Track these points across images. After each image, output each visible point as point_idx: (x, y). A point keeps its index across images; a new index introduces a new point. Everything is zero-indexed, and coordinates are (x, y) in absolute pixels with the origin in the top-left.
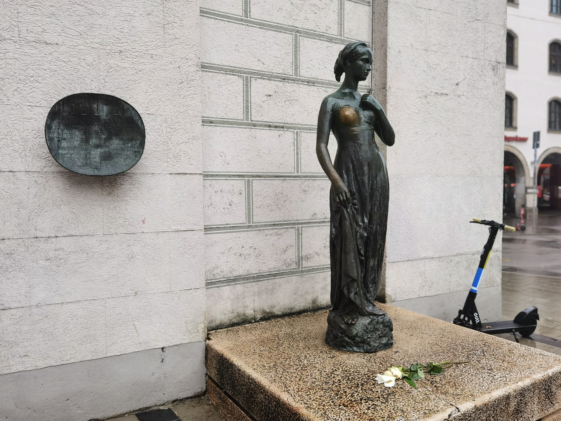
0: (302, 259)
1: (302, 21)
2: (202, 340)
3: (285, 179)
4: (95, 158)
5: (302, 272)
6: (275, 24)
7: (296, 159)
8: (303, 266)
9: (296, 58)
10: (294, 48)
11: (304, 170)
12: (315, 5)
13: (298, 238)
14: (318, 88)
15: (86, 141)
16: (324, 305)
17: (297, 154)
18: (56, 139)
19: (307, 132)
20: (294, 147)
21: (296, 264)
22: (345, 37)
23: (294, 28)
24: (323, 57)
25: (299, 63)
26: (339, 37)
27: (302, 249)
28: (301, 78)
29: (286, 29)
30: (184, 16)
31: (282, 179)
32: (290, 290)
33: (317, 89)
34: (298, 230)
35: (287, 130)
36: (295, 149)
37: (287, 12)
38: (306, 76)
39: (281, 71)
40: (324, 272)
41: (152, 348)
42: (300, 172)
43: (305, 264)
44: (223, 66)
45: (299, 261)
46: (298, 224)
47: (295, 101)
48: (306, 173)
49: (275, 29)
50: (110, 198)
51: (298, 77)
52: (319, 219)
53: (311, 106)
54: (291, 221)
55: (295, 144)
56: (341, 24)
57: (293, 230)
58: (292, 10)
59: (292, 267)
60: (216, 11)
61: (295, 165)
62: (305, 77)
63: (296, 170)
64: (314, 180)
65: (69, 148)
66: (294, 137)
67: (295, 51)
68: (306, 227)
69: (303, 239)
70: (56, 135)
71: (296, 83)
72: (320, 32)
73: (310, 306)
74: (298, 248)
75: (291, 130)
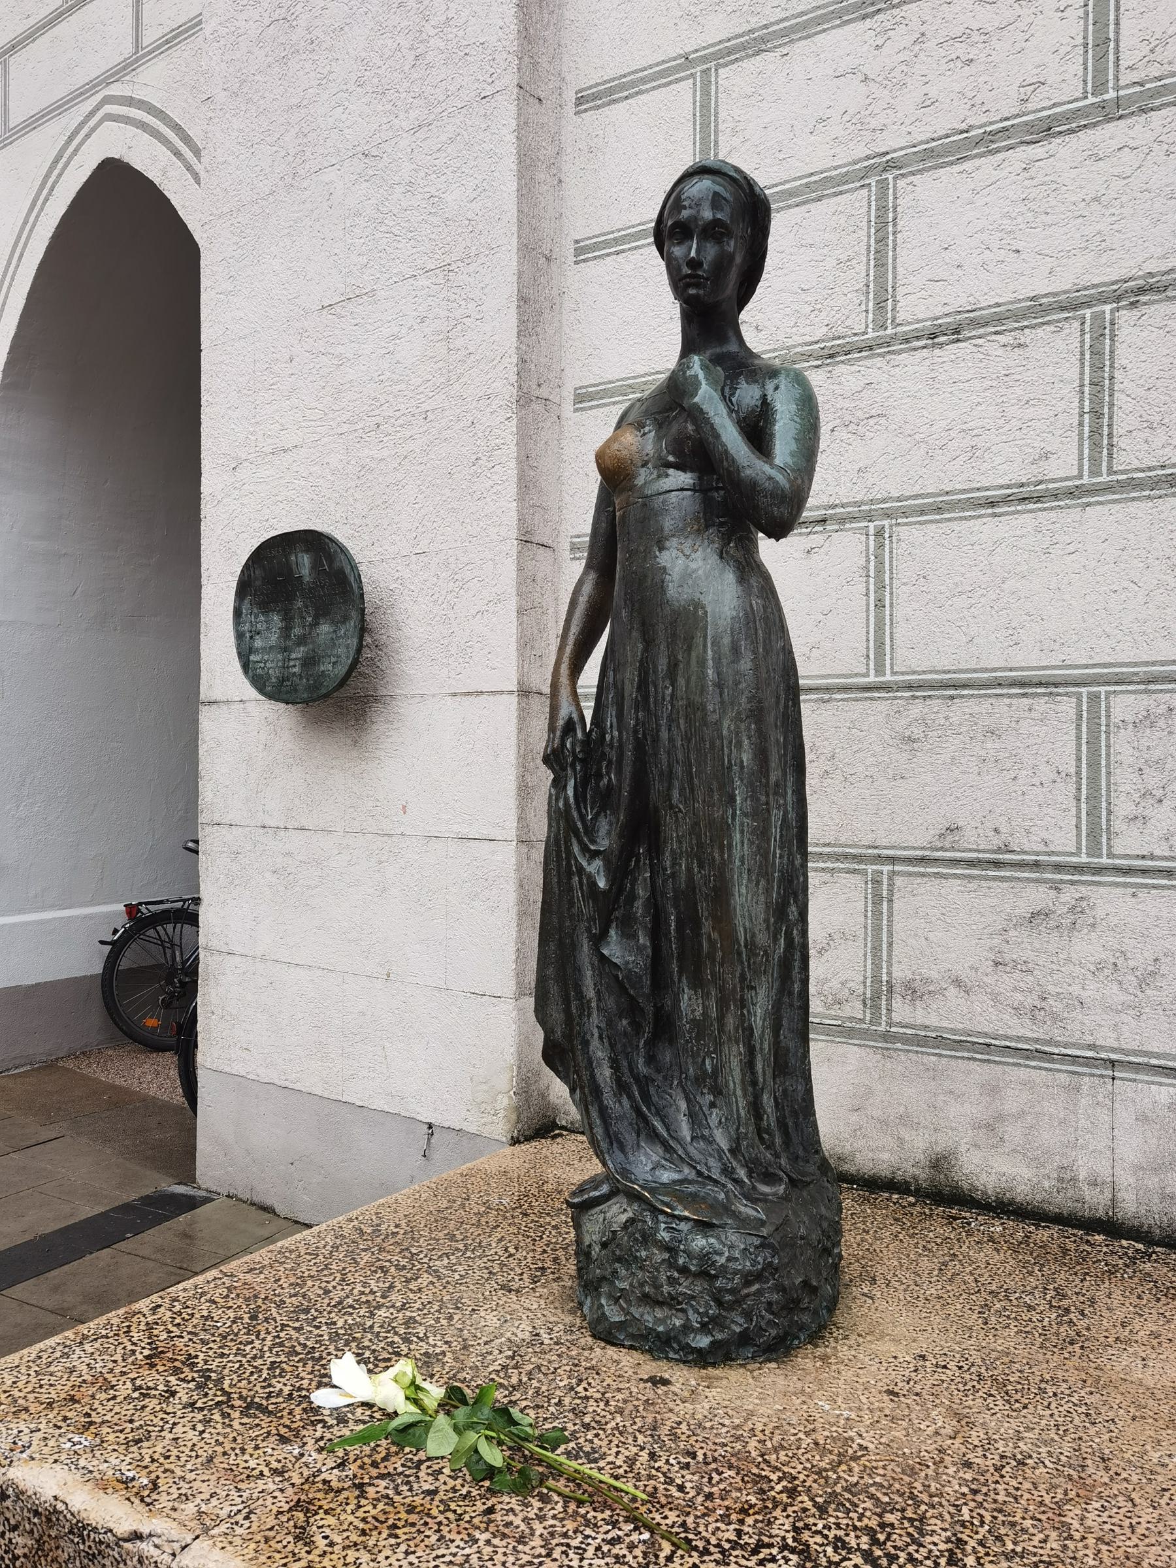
0: (890, 990)
1: (908, 121)
2: (504, 1139)
3: (826, 696)
4: (294, 666)
5: (887, 1037)
6: (798, 183)
7: (872, 626)
8: (896, 1017)
9: (880, 264)
10: (873, 230)
11: (908, 663)
12: (964, 37)
13: (877, 914)
14: (980, 341)
15: (286, 631)
16: (984, 1193)
17: (880, 604)
18: (248, 635)
19: (920, 523)
20: (867, 582)
21: (865, 1004)
22: (1127, 86)
23: (872, 162)
24: (1007, 215)
25: (895, 278)
26: (1091, 100)
27: (890, 955)
28: (899, 329)
29: (845, 179)
30: (485, 291)
31: (813, 697)
32: (835, 1090)
33: (975, 349)
34: (877, 882)
35: (836, 527)
36: (872, 587)
37: (846, 118)
38: (922, 316)
39: (819, 333)
40: (988, 1061)
41: (412, 1115)
42: (888, 672)
43: (902, 1011)
44: (634, 378)
45: (876, 997)
46: (878, 859)
47: (872, 422)
48: (914, 673)
49: (799, 199)
50: (355, 754)
51: (889, 331)
52: (971, 850)
53: (945, 423)
54: (846, 846)
55: (872, 573)
56: (1102, 43)
57: (857, 880)
58: (870, 100)
59: (847, 1011)
60: (619, 230)
61: (868, 648)
62: (919, 321)
63: (872, 666)
64: (952, 698)
65: (264, 650)
66: (867, 549)
67: (877, 241)
68: (910, 874)
69: (896, 918)
70: (247, 627)
71: (879, 355)
72: (991, 123)
73: (923, 1174)
74: (876, 949)
75: (853, 525)
